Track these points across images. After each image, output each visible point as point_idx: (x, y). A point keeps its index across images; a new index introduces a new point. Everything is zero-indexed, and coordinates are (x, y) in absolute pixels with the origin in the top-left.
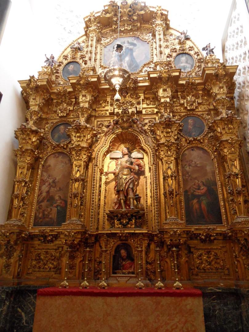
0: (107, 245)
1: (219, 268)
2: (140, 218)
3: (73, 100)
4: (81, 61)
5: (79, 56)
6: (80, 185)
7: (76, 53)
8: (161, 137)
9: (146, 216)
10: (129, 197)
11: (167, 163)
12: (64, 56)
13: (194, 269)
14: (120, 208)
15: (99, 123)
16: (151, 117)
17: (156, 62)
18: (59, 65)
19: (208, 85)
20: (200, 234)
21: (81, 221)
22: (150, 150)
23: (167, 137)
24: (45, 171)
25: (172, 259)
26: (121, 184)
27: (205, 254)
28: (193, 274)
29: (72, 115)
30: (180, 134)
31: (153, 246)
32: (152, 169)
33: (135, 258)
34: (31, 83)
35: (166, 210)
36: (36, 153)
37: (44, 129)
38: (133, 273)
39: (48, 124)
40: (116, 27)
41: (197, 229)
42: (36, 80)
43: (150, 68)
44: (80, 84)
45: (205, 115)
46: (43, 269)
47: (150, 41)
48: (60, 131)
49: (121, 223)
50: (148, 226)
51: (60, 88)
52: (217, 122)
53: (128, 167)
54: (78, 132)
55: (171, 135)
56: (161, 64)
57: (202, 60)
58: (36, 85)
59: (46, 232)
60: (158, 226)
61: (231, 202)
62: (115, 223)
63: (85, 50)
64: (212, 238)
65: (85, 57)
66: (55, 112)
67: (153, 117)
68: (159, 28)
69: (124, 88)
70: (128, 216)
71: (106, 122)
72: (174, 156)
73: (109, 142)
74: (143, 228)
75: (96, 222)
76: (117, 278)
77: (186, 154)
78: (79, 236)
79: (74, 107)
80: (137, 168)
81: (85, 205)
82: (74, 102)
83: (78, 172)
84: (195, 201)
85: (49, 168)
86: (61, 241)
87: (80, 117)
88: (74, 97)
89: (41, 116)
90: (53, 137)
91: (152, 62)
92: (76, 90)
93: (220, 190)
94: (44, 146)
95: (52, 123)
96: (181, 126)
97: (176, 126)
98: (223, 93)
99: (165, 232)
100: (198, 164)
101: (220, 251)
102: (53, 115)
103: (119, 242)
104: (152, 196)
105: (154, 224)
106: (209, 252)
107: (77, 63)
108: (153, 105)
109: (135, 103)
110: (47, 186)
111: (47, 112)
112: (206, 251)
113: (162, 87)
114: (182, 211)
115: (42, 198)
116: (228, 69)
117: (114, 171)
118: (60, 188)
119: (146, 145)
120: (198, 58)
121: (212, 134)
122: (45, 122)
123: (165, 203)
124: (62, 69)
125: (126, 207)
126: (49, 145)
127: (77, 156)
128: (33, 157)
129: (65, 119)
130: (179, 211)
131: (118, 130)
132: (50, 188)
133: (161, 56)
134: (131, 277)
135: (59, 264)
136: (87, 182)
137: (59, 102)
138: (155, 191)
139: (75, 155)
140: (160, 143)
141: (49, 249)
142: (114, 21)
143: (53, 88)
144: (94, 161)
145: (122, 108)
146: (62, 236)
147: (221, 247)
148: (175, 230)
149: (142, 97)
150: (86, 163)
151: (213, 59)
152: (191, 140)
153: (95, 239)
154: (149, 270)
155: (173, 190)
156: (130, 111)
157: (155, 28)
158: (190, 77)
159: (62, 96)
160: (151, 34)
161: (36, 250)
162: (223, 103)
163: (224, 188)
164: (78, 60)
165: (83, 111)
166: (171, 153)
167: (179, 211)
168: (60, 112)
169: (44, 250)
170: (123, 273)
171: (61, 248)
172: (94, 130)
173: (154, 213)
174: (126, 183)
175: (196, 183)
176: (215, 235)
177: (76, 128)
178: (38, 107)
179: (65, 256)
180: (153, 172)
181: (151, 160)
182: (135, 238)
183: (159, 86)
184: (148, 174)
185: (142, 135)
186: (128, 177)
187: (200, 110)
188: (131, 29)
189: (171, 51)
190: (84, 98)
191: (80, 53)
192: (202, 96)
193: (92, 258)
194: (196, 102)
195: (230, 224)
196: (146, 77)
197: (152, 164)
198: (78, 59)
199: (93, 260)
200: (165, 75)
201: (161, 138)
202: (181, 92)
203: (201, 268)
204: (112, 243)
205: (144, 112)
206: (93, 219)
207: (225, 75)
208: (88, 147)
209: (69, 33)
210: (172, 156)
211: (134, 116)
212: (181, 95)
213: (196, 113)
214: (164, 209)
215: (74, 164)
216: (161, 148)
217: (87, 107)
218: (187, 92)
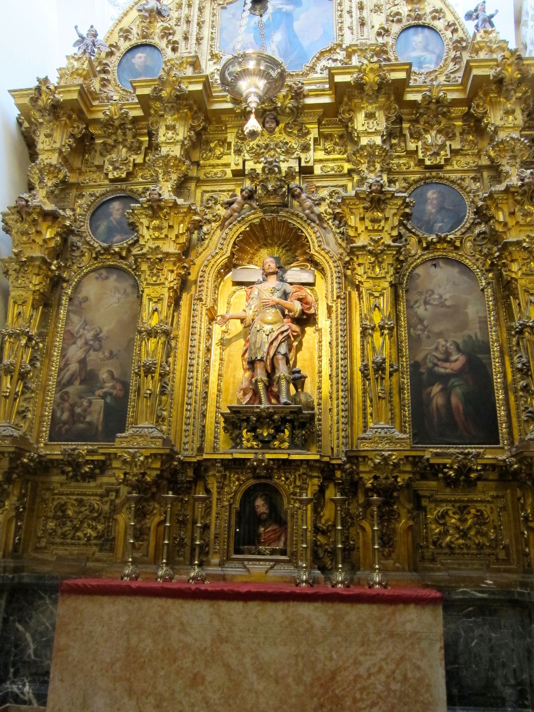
0: (222, 488)
1: (484, 545)
2: (303, 426)
3: (142, 139)
4: (162, 44)
5: (158, 31)
6: (160, 346)
7: (150, 22)
8: (359, 231)
9: (316, 423)
10: (278, 375)
11: (371, 295)
12: (121, 30)
13: (427, 547)
14: (255, 401)
15: (207, 196)
16: (335, 183)
17: (350, 46)
18: (111, 54)
19: (478, 106)
20: (444, 466)
21: (161, 431)
22: (332, 265)
23: (374, 231)
24: (75, 313)
26: (258, 346)
27: (454, 513)
28: (423, 558)
29: (142, 177)
30: (405, 226)
31: (331, 493)
32: (334, 309)
33: (289, 518)
34: (41, 95)
35: (365, 409)
36: (53, 267)
37: (73, 210)
38: (283, 552)
39: (82, 198)
41: (437, 455)
42: (52, 87)
43: (335, 60)
44: (159, 99)
45: (467, 181)
46: (73, 538)
48: (111, 214)
50: (320, 447)
51: (111, 110)
52: (496, 196)
53: (278, 304)
54: (154, 216)
55: (383, 228)
56: (361, 50)
57: (464, 44)
58: (52, 100)
59: (79, 455)
60: (346, 445)
61: (521, 393)
62: (243, 437)
63: (175, 15)
64: (472, 475)
65: (173, 34)
66: (100, 168)
67: (340, 183)
69: (270, 110)
70: (273, 421)
71: (225, 193)
72: (389, 279)
74: (309, 450)
75: (198, 433)
76: (246, 563)
77: (418, 274)
78: (158, 465)
79: (146, 156)
81: (172, 394)
82: (146, 145)
83: (156, 313)
84: (436, 389)
85: (84, 305)
86: (114, 476)
87: (160, 179)
88: (146, 131)
89: (65, 177)
90: (94, 228)
91: (340, 46)
92: (150, 115)
93: (496, 364)
94: (74, 251)
95: (91, 195)
96: (407, 205)
97: (395, 204)
98: (515, 127)
99: (361, 459)
100: (446, 300)
101: (489, 506)
102: (95, 176)
103: (252, 482)
104: (334, 374)
106: (463, 509)
108: (339, 154)
109: (295, 146)
110: (81, 348)
111: (80, 169)
112: (457, 505)
113: (363, 108)
114: (404, 411)
116: (528, 65)
117: (243, 314)
118: (111, 353)
119: (322, 253)
120: (456, 37)
121: (483, 228)
122: (74, 192)
123: (364, 392)
124: (117, 63)
125: (270, 401)
126: (85, 250)
127: (153, 275)
128: (47, 276)
129: (124, 187)
130: (397, 411)
131: (253, 214)
132: (87, 351)
133: (362, 32)
134: (277, 562)
135: (108, 529)
136: (176, 338)
137: (110, 145)
138: (340, 362)
139: (148, 272)
140: (354, 245)
141: (85, 494)
143: (94, 109)
144: (193, 288)
145: (263, 159)
146: (116, 464)
147: (493, 497)
148: (386, 454)
149: (314, 133)
150: (175, 291)
151: (490, 41)
153: (195, 473)
154: (321, 546)
156: (284, 167)
158: (432, 85)
159: (117, 129)
161: (56, 497)
162: (513, 151)
163: (507, 358)
164: (156, 40)
165: (167, 165)
166: (383, 271)
167: (397, 411)
168: (111, 168)
169: (74, 497)
170: (260, 553)
172: (196, 213)
173: (338, 414)
174: (272, 343)
175: (440, 347)
176: (479, 468)
177: (151, 207)
178: (57, 155)
179: (124, 510)
180: (337, 318)
181: (332, 288)
182: (290, 473)
183: (355, 105)
184: (323, 321)
185: (312, 228)
186: (275, 327)
187: (456, 167)
189: (387, 20)
190: (170, 134)
191: (162, 23)
192: (461, 134)
193: (186, 516)
194: (448, 148)
195: (517, 443)
196: (325, 83)
197: (335, 298)
198: (156, 38)
199: (190, 520)
200: (371, 78)
201: (359, 234)
202: (410, 121)
203: (443, 545)
204: (234, 482)
205: (317, 171)
206: (190, 428)
207: (520, 82)
208: (179, 254)
210: (385, 277)
211: (294, 178)
212: (409, 128)
213: (447, 175)
214: (361, 405)
215: (145, 295)
216: (357, 258)
217: (178, 155)
218: (425, 123)
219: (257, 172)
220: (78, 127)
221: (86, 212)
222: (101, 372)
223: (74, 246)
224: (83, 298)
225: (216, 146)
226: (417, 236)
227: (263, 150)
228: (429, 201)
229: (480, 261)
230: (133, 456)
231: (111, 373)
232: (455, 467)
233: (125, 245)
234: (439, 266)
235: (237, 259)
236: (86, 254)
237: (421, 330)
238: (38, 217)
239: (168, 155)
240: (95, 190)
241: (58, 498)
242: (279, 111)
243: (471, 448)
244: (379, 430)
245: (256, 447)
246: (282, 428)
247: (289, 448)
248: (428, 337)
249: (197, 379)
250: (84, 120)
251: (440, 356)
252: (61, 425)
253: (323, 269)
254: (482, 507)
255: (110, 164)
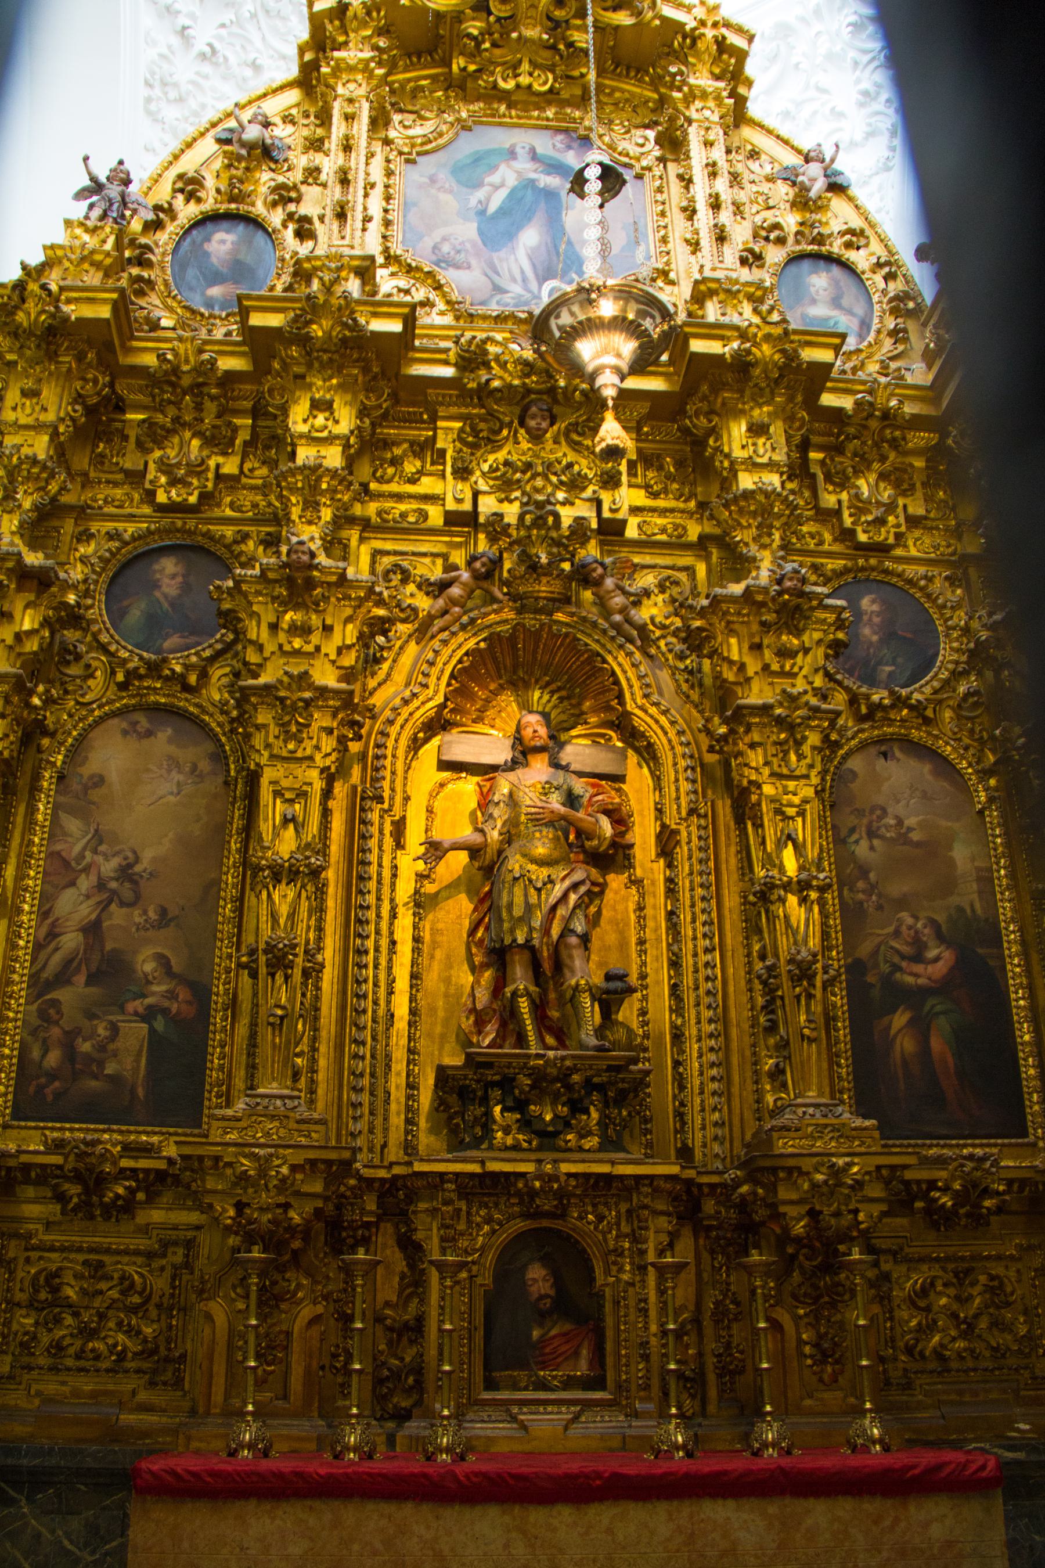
3: (238, 421)
4: (276, 218)
5: (263, 190)
7: (247, 169)
10: (573, 982)
12: (181, 177)
13: (896, 1359)
14: (504, 1039)
15: (387, 561)
16: (667, 561)
18: (154, 226)
20: (932, 1185)
23: (782, 674)
24: (73, 812)
25: (801, 1312)
26: (518, 912)
29: (232, 506)
33: (608, 1307)
34: (23, 301)
36: (36, 701)
38: (597, 1382)
39: (88, 542)
40: (472, 68)
44: (304, 341)
45: (938, 583)
47: (649, 169)
48: (156, 585)
49: (526, 1124)
56: (728, 291)
57: (911, 305)
62: (495, 1122)
63: (301, 161)
64: (987, 1203)
65: (298, 200)
66: (136, 477)
68: (707, 113)
69: (539, 392)
70: (569, 1087)
71: (427, 560)
73: (447, 673)
76: (515, 1410)
77: (852, 771)
80: (606, 827)
83: (291, 826)
84: (900, 1019)
85: (95, 795)
87: (294, 517)
88: (248, 404)
90: (117, 615)
93: (1014, 966)
94: (68, 663)
95: (110, 536)
99: (782, 1175)
100: (910, 829)
102: (118, 493)
103: (520, 1225)
105: (699, 1135)
106: (963, 1276)
107: (255, 223)
108: (677, 499)
110: (88, 897)
111: (86, 475)
112: (951, 1266)
113: (743, 412)
114: (839, 1065)
115: (57, 958)
118: (163, 912)
119: (653, 710)
122: (69, 527)
124: (170, 248)
125: (541, 1039)
126: (95, 664)
127: (288, 736)
128: (18, 721)
129: (191, 524)
131: (496, 612)
132: (105, 905)
133: (720, 254)
134: (587, 1404)
137: (163, 427)
139: (274, 730)
141: (108, 1251)
142: (469, 36)
143: (135, 344)
145: (517, 494)
147: (1019, 1247)
148: (841, 1162)
152: (880, 706)
155: (815, 955)
156: (567, 515)
157: (681, 106)
159: (185, 394)
160: (651, 134)
161: (34, 1255)
164: (259, 209)
166: (804, 762)
168: (163, 480)
169: (81, 1257)
170: (542, 1386)
171: (180, 1251)
175: (904, 928)
177: (290, 582)
178: (46, 438)
182: (606, 1204)
183: (724, 404)
185: (630, 654)
187: (914, 552)
188: (551, 90)
189: (755, 236)
191: (272, 175)
194: (900, 510)
197: (684, 814)
198: (259, 204)
201: (748, 680)
202: (820, 448)
204: (479, 1226)
205: (632, 532)
209: (203, 56)
210: (807, 777)
211: (584, 542)
212: (822, 463)
215: (264, 781)
218: (855, 455)
219: (506, 520)
220: (95, 381)
221: (100, 575)
222: (141, 958)
223: (70, 653)
224: (92, 777)
225: (405, 453)
226: (847, 689)
227: (518, 475)
228: (865, 618)
229: (971, 751)
230: (264, 1165)
231: (163, 961)
232: (957, 1186)
233: (194, 659)
234: (893, 757)
235: (452, 711)
236: (98, 673)
237: (863, 892)
238: (9, 579)
239: (320, 465)
240: (120, 526)
241: (41, 1258)
242: (560, 397)
243: (974, 1146)
244: (811, 1110)
245: (525, 1145)
246: (586, 1102)
247: (602, 1148)
248: (880, 908)
249: (376, 985)
250: (108, 367)
251: (905, 949)
252: (43, 1080)
253: (650, 745)
254: (998, 1270)
255: (160, 470)
